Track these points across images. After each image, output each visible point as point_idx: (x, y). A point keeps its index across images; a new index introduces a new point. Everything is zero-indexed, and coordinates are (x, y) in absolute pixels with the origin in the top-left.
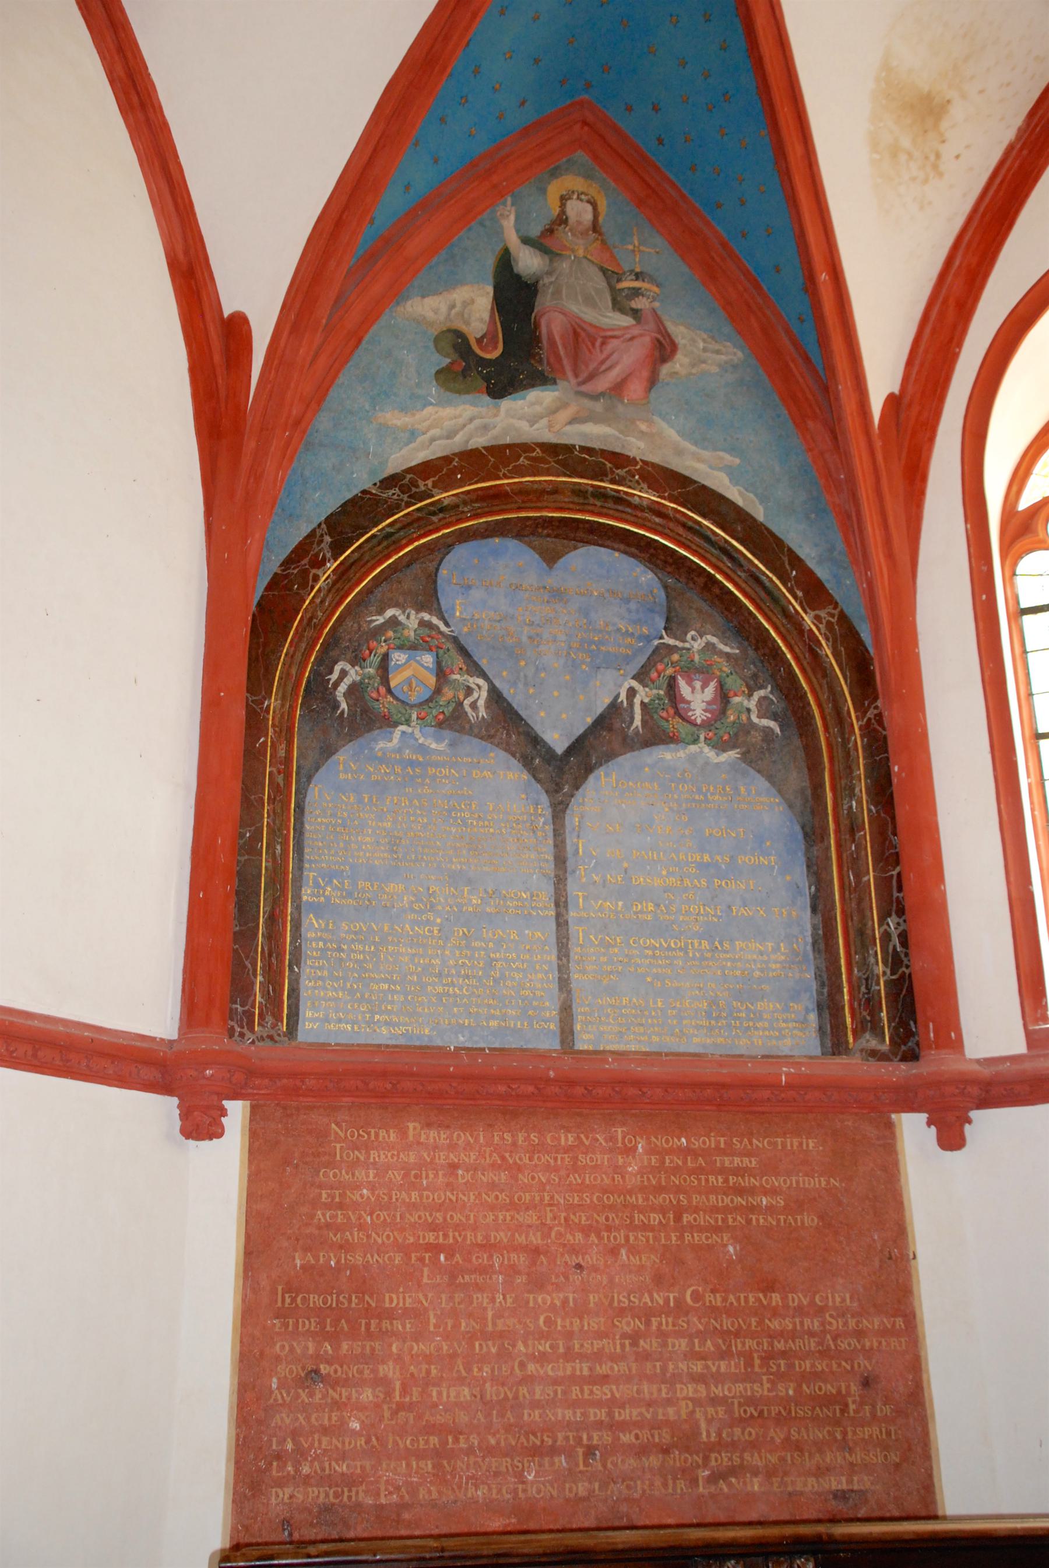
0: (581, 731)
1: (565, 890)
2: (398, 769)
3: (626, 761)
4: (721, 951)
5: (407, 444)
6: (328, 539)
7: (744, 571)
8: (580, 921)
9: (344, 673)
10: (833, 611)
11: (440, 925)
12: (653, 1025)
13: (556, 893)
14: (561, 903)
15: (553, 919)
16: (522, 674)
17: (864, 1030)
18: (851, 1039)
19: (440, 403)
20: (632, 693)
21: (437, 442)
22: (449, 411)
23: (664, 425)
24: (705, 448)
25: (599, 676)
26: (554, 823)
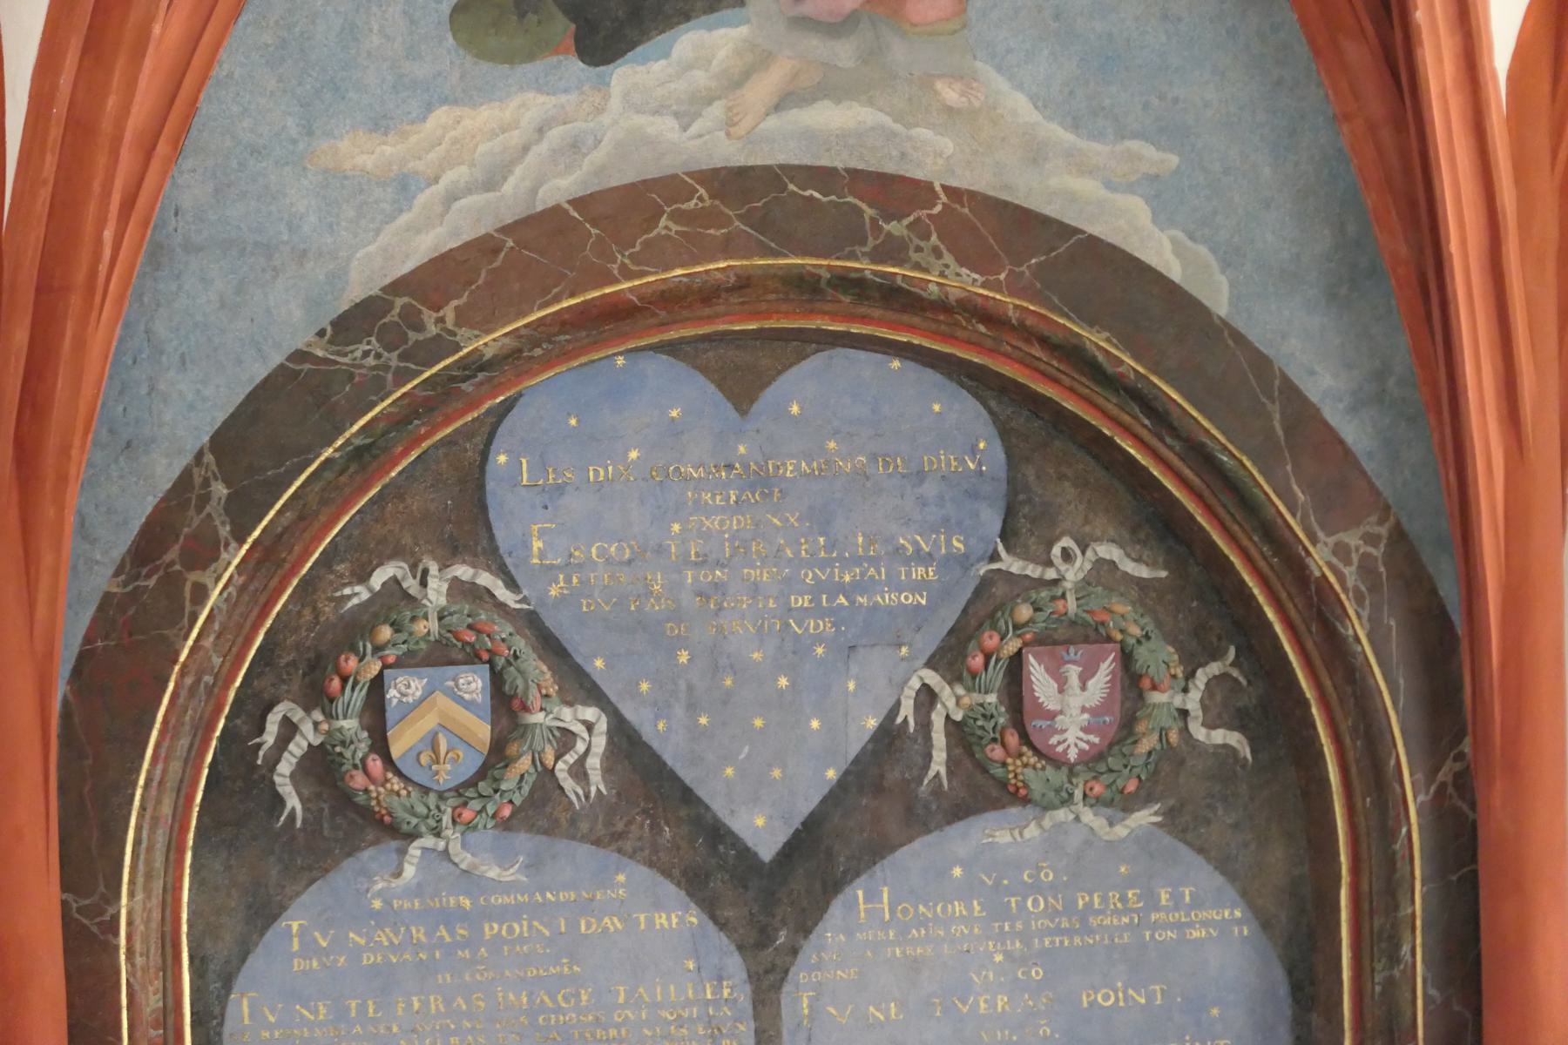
0: (815, 800)
2: (419, 933)
3: (913, 856)
5: (391, 218)
6: (220, 490)
19: (467, 96)
20: (927, 697)
21: (463, 202)
22: (485, 116)
23: (1000, 83)
24: (1097, 136)
25: (854, 669)
26: (756, 1017)
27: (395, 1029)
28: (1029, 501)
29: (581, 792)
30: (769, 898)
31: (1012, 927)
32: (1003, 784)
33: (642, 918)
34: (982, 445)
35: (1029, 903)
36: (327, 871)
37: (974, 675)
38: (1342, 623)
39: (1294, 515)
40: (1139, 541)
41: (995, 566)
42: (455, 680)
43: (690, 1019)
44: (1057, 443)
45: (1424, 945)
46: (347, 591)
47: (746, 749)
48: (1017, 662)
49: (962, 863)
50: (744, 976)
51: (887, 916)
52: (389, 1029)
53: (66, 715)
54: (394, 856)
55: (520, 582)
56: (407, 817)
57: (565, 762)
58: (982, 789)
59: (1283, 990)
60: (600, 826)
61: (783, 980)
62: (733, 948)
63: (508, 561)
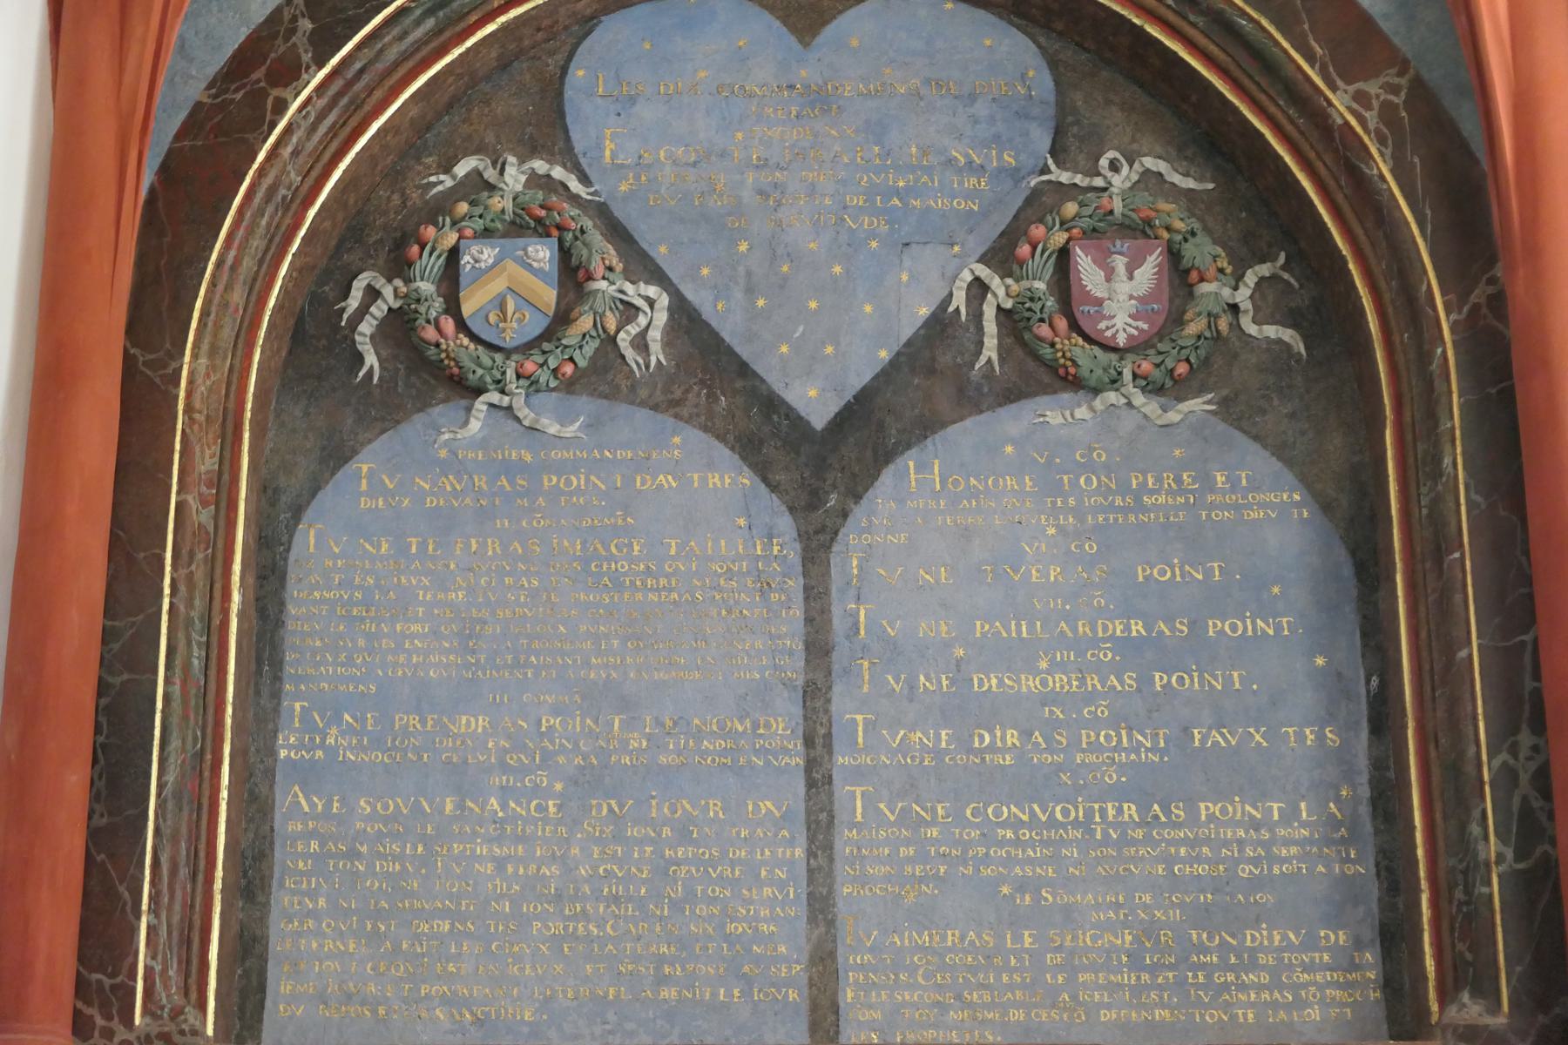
0: (867, 378)
1: (827, 711)
2: (481, 482)
3: (965, 434)
4: (1164, 825)
6: (306, 25)
7: (1202, 13)
8: (858, 775)
9: (373, 294)
10: (1397, 80)
11: (561, 795)
12: (1011, 987)
13: (806, 718)
14: (817, 742)
15: (802, 773)
16: (741, 269)
17: (1458, 988)
18: (1435, 1007)
20: (979, 289)
25: (907, 263)
26: (805, 574)
27: (452, 566)
28: (1077, 122)
29: (641, 361)
30: (820, 465)
31: (1065, 502)
32: (1052, 367)
33: (696, 477)
34: (1031, 74)
35: (1082, 480)
36: (398, 422)
37: (1021, 263)
38: (1367, 164)
39: (1312, 67)
40: (1186, 158)
41: (1045, 178)
42: (525, 250)
43: (739, 572)
44: (1104, 74)
45: (1464, 453)
46: (433, 179)
47: (801, 329)
48: (1064, 254)
49: (1014, 442)
50: (795, 535)
51: (938, 487)
52: (447, 566)
53: (152, 191)
54: (462, 413)
55: (593, 178)
56: (473, 367)
57: (628, 332)
58: (1037, 369)
59: (1348, 571)
60: (658, 393)
61: (832, 540)
62: (784, 508)
63: (583, 161)
